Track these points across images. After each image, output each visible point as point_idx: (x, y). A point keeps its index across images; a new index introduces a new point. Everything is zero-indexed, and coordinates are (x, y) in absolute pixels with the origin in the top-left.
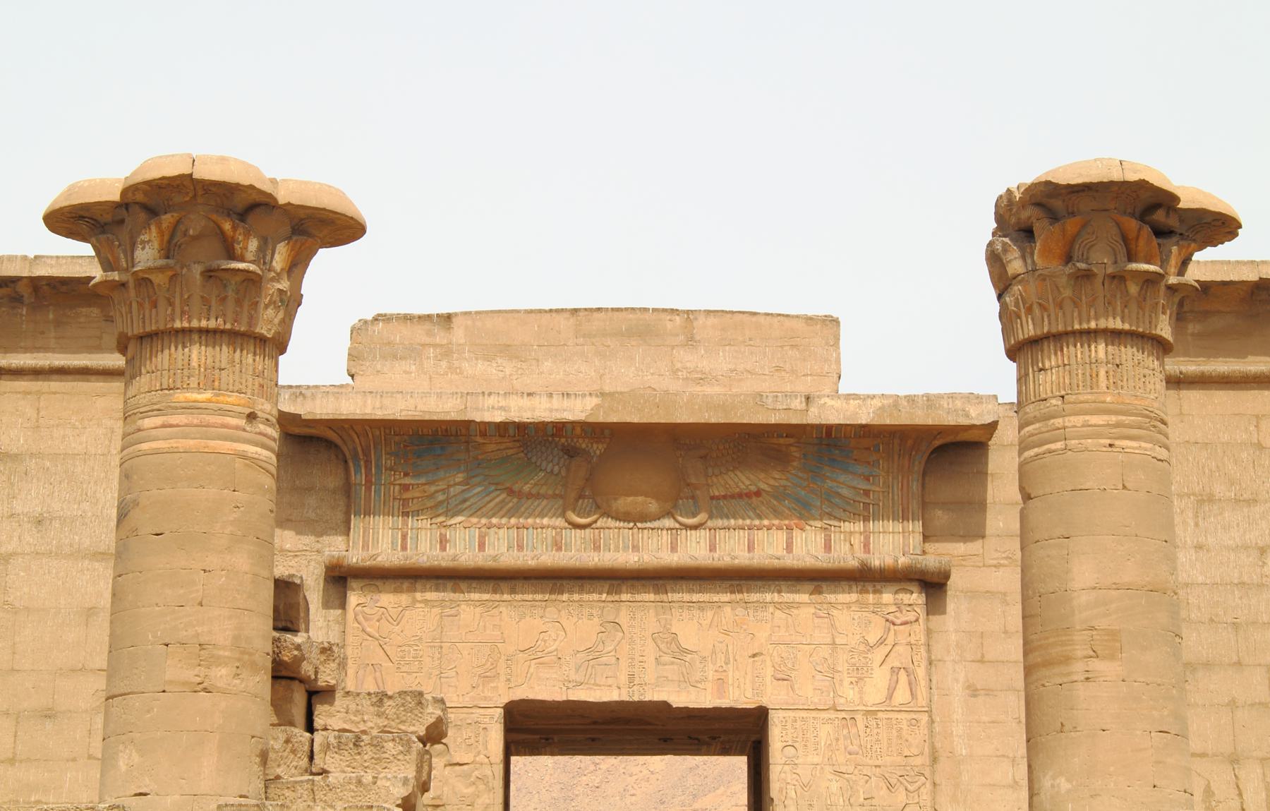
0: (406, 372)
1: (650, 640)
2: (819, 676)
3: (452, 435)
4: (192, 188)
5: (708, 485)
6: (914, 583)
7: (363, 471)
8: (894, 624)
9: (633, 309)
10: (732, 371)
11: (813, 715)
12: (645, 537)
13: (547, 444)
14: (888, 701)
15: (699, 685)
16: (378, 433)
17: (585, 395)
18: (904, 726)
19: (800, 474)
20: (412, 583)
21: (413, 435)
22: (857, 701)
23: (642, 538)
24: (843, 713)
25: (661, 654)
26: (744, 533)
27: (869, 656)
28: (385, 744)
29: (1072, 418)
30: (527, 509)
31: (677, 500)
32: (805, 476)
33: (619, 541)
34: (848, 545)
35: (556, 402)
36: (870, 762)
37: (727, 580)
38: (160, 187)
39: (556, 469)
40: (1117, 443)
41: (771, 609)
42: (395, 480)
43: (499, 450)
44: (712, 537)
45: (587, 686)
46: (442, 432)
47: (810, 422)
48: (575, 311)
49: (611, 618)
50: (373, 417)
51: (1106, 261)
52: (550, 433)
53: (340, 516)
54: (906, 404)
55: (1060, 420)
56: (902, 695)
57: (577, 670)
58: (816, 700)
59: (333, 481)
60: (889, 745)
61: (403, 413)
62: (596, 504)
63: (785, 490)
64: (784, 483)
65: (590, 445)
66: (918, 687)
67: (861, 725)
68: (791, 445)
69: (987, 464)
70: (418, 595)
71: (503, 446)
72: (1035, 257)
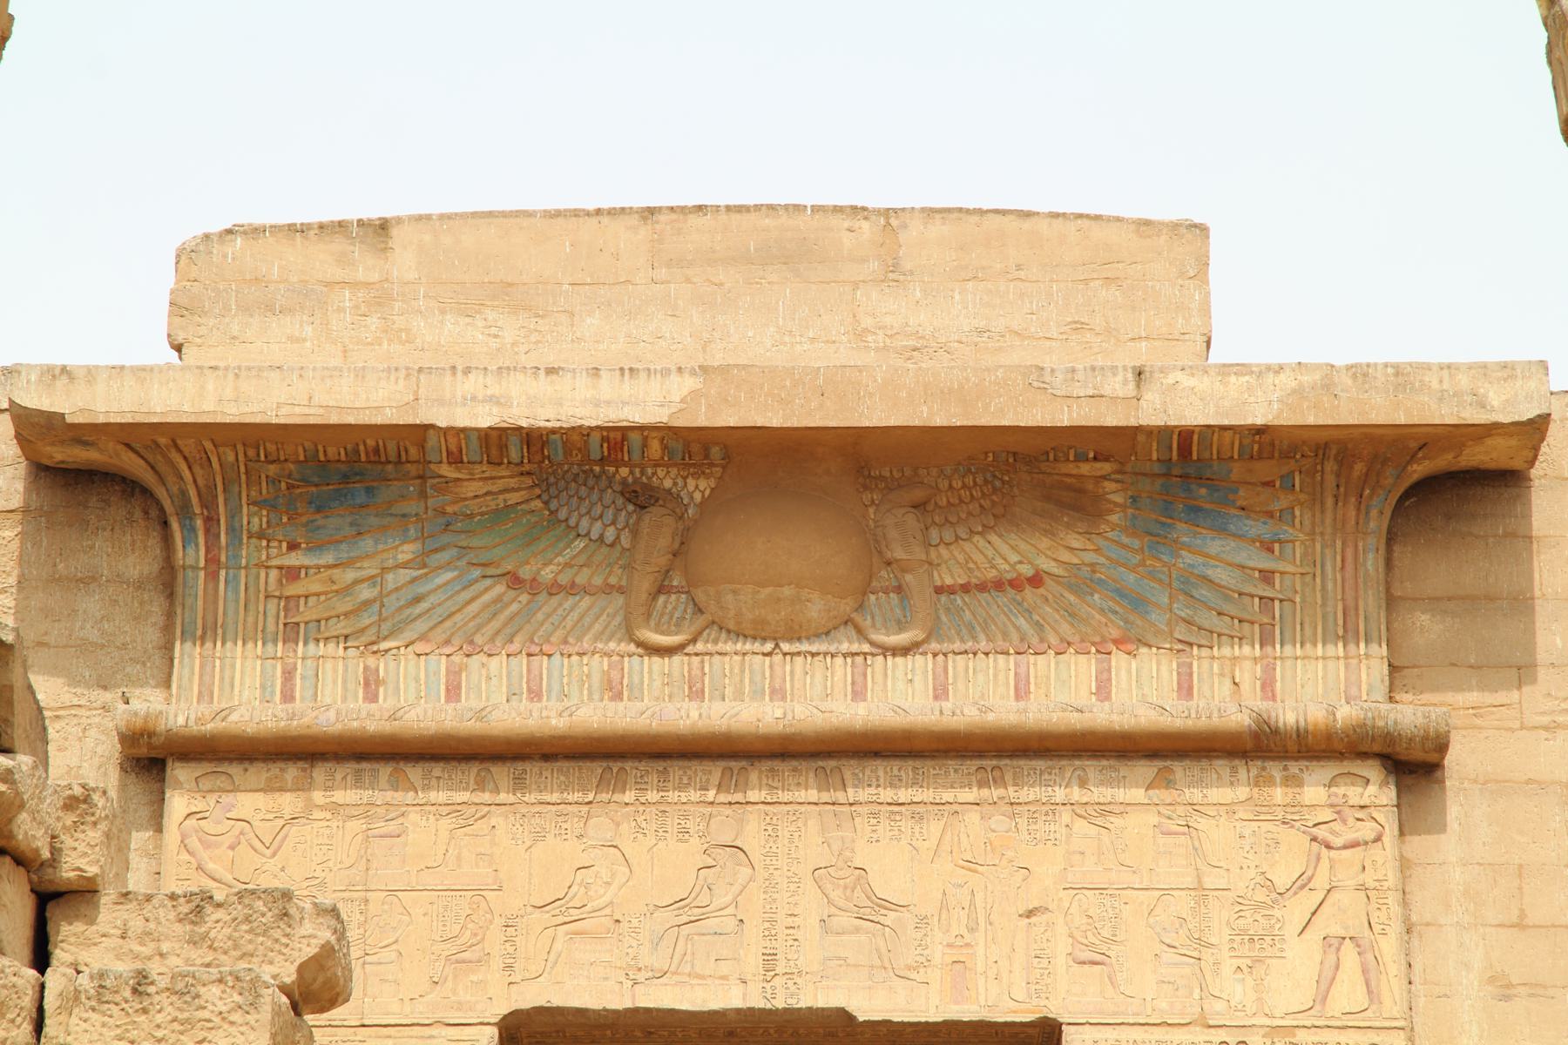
0: (293, 339)
2: (1169, 956)
3: (390, 462)
5: (930, 564)
6: (1370, 762)
7: (201, 540)
8: (1328, 847)
9: (771, 207)
10: (981, 332)
11: (1157, 1037)
13: (591, 482)
14: (1318, 1007)
15: (913, 975)
16: (231, 458)
17: (669, 371)
19: (1125, 540)
20: (304, 770)
21: (306, 461)
23: (792, 672)
24: (1220, 1031)
25: (833, 910)
26: (1008, 661)
27: (1277, 913)
30: (549, 616)
31: (864, 594)
32: (1136, 543)
33: (742, 681)
34: (1228, 682)
35: (608, 387)
37: (972, 757)
39: (610, 534)
42: (268, 557)
43: (488, 493)
44: (940, 670)
45: (675, 978)
46: (367, 454)
47: (1144, 422)
48: (651, 211)
50: (219, 419)
52: (596, 455)
53: (153, 635)
54: (1350, 382)
56: (1348, 995)
57: (656, 946)
58: (1164, 1005)
59: (139, 562)
61: (284, 411)
62: (695, 604)
63: (1094, 572)
64: (1090, 557)
65: (680, 481)
66: (1383, 977)
68: (1104, 478)
69: (1527, 516)
70: (318, 796)
71: (500, 484)
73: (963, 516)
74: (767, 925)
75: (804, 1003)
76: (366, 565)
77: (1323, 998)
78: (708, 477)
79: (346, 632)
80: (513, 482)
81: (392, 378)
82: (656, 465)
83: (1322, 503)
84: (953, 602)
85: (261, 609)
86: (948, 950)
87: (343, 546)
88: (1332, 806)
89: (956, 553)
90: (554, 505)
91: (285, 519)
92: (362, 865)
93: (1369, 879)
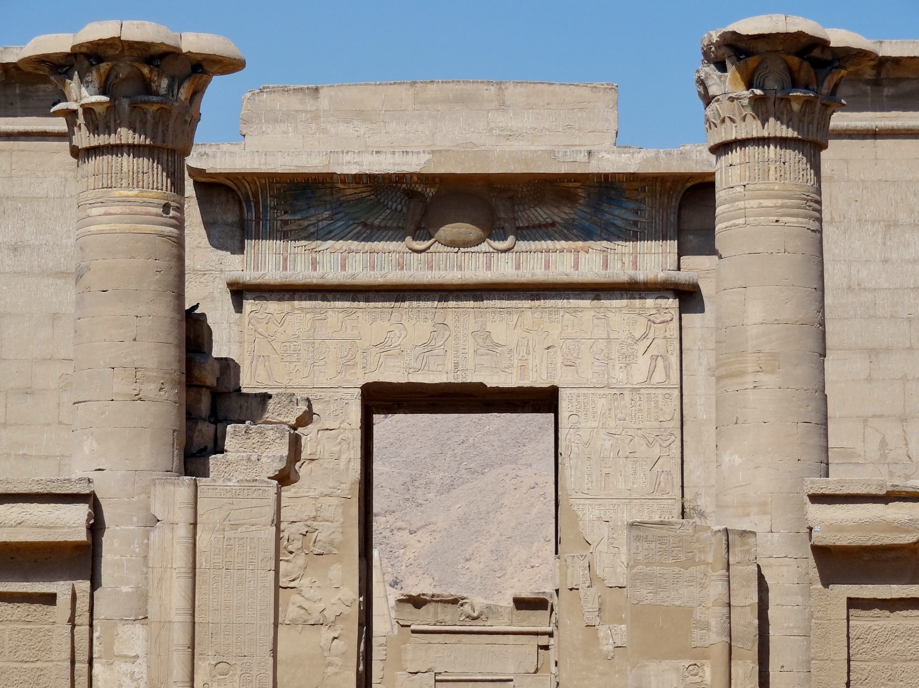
1: (470, 339)
3: (319, 183)
4: (121, 45)
6: (671, 292)
7: (253, 210)
8: (654, 323)
13: (392, 189)
15: (507, 370)
17: (420, 152)
18: (660, 399)
22: (625, 381)
24: (615, 390)
25: (478, 347)
28: (267, 432)
29: (751, 202)
32: (588, 211)
35: (398, 158)
36: (635, 426)
38: (98, 45)
39: (399, 207)
40: (781, 219)
43: (355, 193)
44: (517, 258)
51: (776, 88)
53: (237, 243)
54: (664, 156)
55: (742, 203)
56: (659, 376)
58: (595, 381)
60: (649, 413)
63: (574, 221)
64: (573, 216)
65: (424, 189)
68: (578, 188)
73: (527, 201)
74: (455, 352)
75: (469, 380)
76: (312, 219)
77: (650, 376)
78: (434, 188)
80: (364, 189)
81: (321, 156)
82: (416, 183)
83: (656, 196)
84: (523, 233)
85: (275, 235)
86: (519, 361)
87: (304, 212)
88: (656, 308)
89: (524, 214)
90: (379, 197)
91: (283, 203)
92: (312, 331)
93: (668, 334)
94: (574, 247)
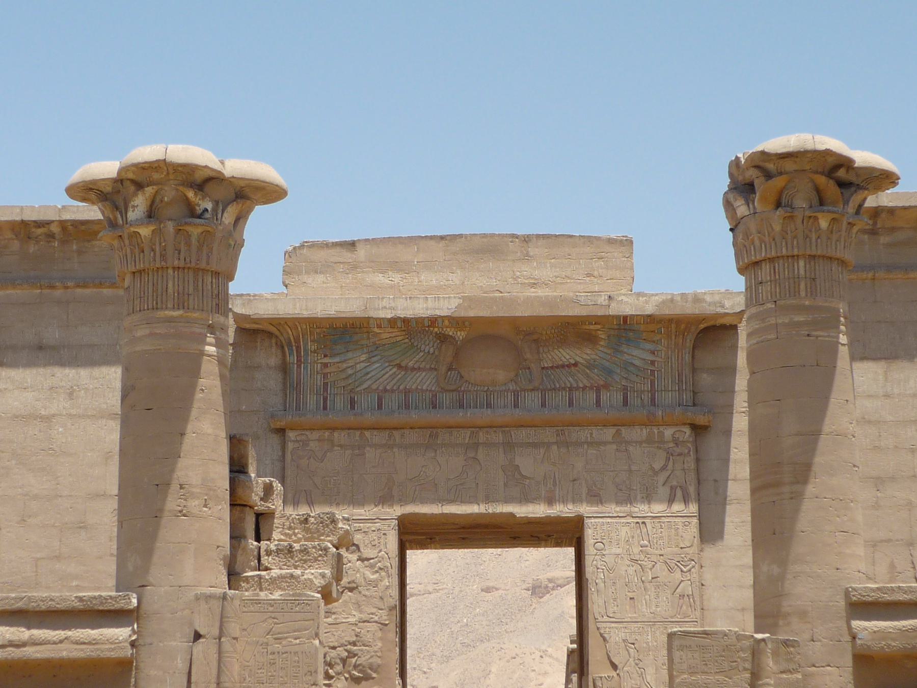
12: (495, 397)
16: (305, 327)
19: (605, 350)
27: (655, 478)
32: (609, 352)
33: (477, 401)
34: (639, 400)
39: (432, 350)
41: (586, 446)
42: (317, 360)
49: (472, 455)
51: (804, 206)
64: (594, 357)
65: (455, 333)
67: (649, 526)
69: (737, 339)
72: (756, 204)
76: (350, 361)
79: (344, 385)
80: (399, 333)
89: (549, 355)
90: (413, 341)
94: (596, 385)
